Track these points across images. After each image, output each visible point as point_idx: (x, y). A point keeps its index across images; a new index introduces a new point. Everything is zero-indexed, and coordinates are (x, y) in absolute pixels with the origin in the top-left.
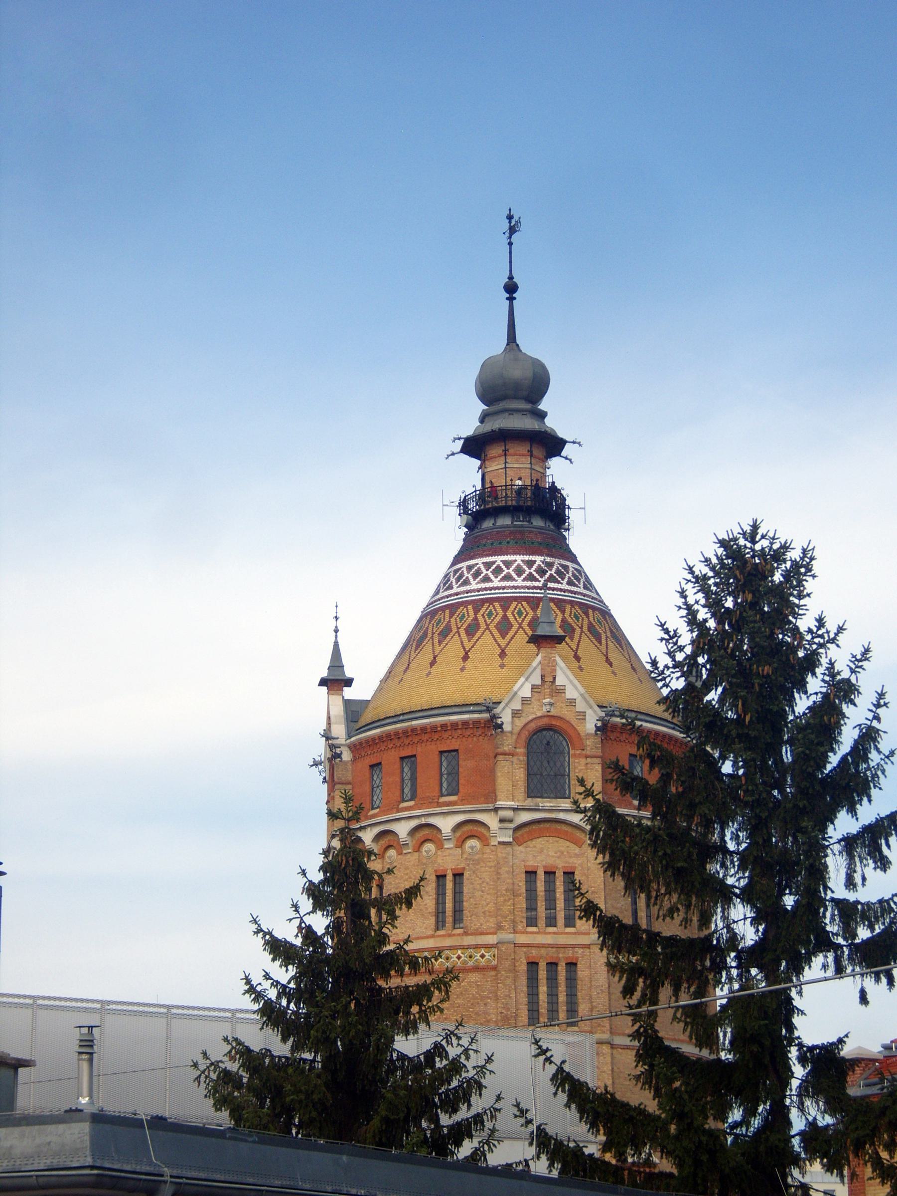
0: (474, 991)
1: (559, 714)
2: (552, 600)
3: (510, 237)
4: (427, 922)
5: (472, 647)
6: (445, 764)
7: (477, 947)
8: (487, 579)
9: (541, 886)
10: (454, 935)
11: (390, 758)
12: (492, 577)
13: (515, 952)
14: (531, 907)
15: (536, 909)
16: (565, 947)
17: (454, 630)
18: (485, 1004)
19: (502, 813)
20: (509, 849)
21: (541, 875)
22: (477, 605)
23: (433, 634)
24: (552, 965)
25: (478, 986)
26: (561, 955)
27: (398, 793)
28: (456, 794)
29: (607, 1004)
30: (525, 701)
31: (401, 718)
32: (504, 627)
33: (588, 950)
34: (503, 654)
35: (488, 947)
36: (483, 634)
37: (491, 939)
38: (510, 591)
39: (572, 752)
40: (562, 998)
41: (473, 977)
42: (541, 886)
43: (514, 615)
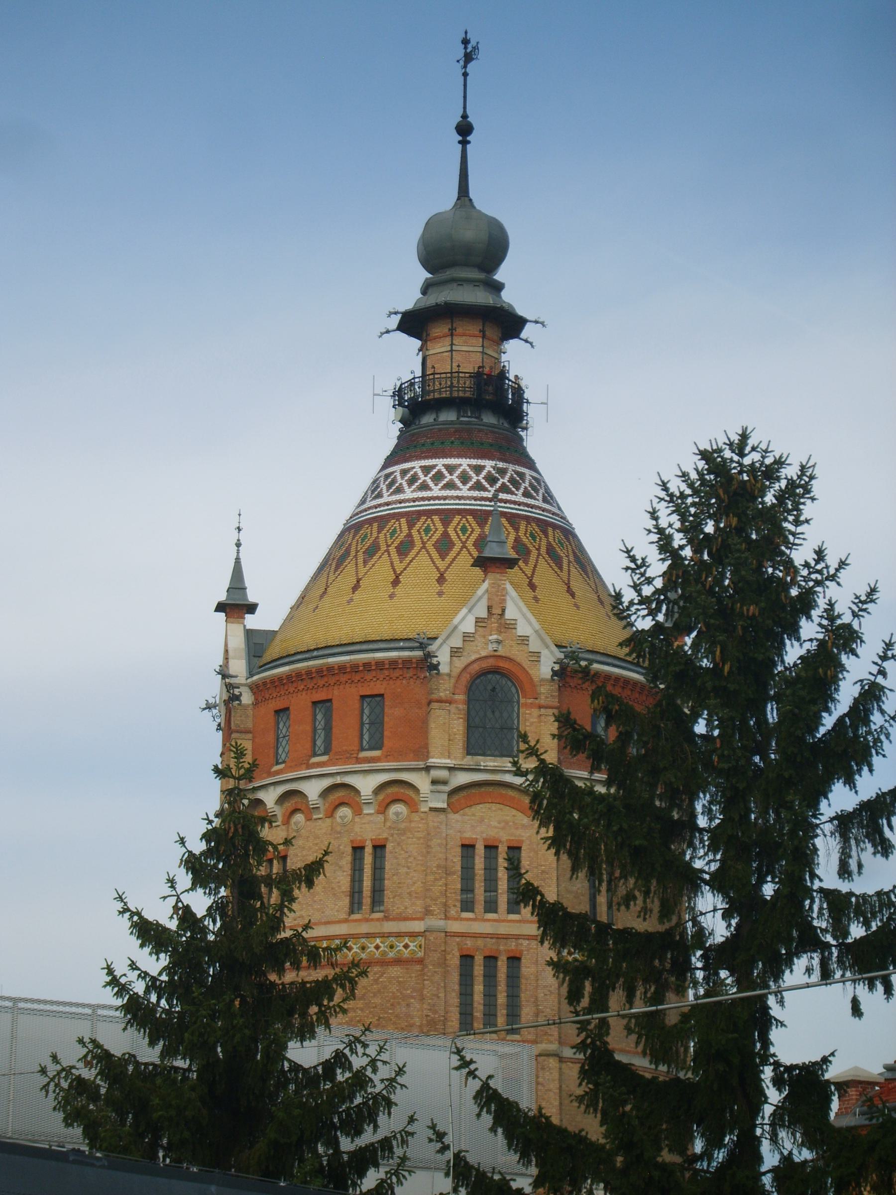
0: (394, 988)
1: (507, 655)
2: (504, 514)
3: (465, 67)
4: (340, 903)
5: (405, 569)
6: (367, 711)
7: (399, 935)
8: (424, 487)
9: (479, 863)
10: (372, 920)
11: (300, 702)
12: (431, 484)
13: (445, 942)
14: (467, 888)
15: (472, 891)
16: (507, 937)
17: (383, 548)
18: (408, 1005)
19: (435, 773)
20: (442, 816)
21: (480, 850)
22: (412, 518)
23: (357, 552)
24: (491, 960)
25: (399, 982)
26: (501, 948)
27: (308, 745)
28: (380, 748)
29: (556, 1008)
30: (466, 637)
31: (315, 653)
32: (444, 546)
34: (441, 579)
35: (413, 935)
36: (418, 553)
37: (418, 926)
38: (452, 502)
39: (522, 701)
40: (502, 999)
41: (395, 971)
42: (479, 863)
43: (456, 532)
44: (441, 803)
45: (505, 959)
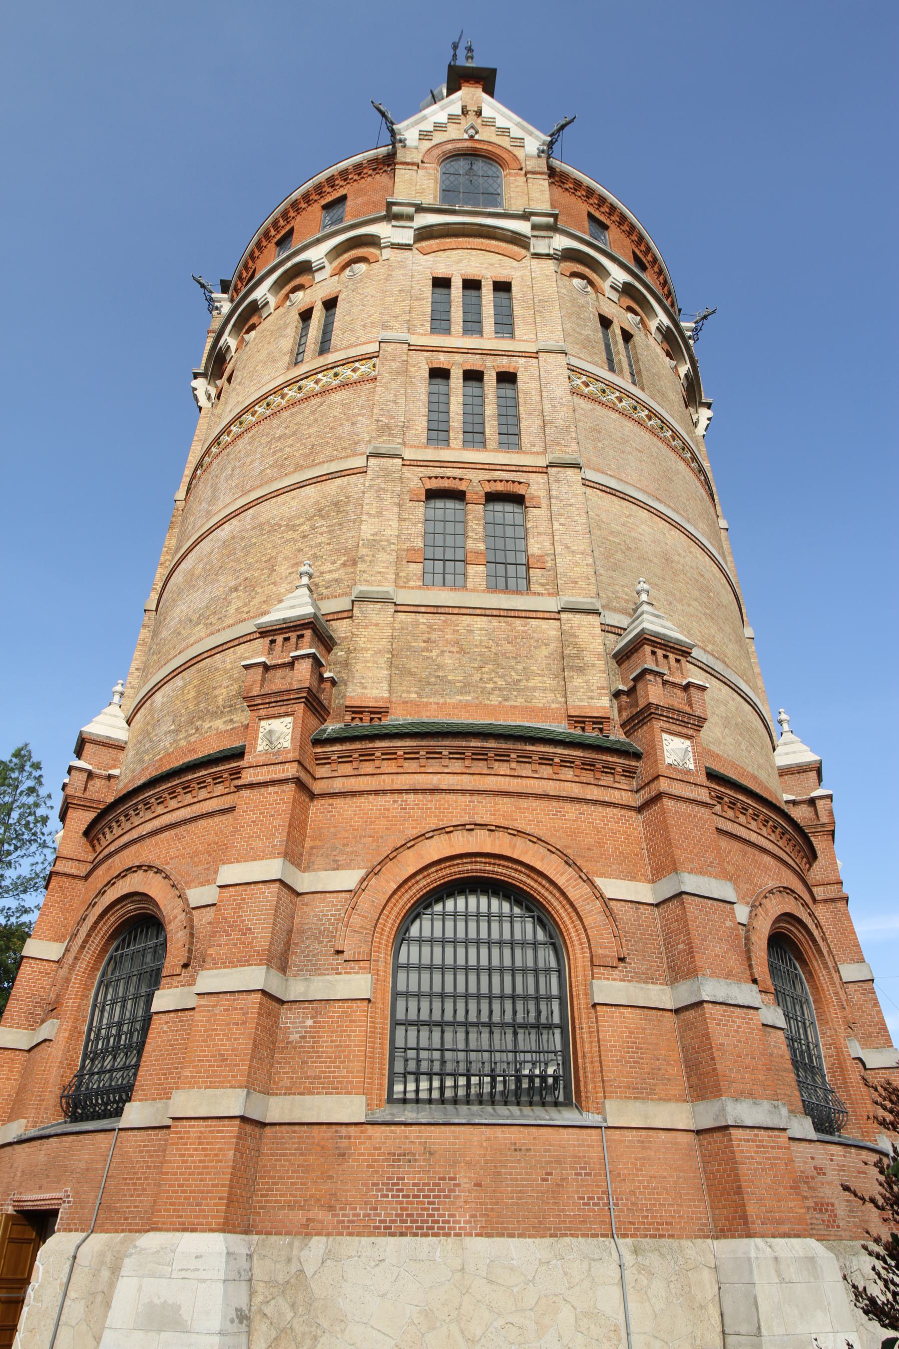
7: (345, 363)
20: (408, 254)
26: (488, 364)
30: (439, 127)
33: (536, 360)
41: (336, 397)
44: (406, 236)
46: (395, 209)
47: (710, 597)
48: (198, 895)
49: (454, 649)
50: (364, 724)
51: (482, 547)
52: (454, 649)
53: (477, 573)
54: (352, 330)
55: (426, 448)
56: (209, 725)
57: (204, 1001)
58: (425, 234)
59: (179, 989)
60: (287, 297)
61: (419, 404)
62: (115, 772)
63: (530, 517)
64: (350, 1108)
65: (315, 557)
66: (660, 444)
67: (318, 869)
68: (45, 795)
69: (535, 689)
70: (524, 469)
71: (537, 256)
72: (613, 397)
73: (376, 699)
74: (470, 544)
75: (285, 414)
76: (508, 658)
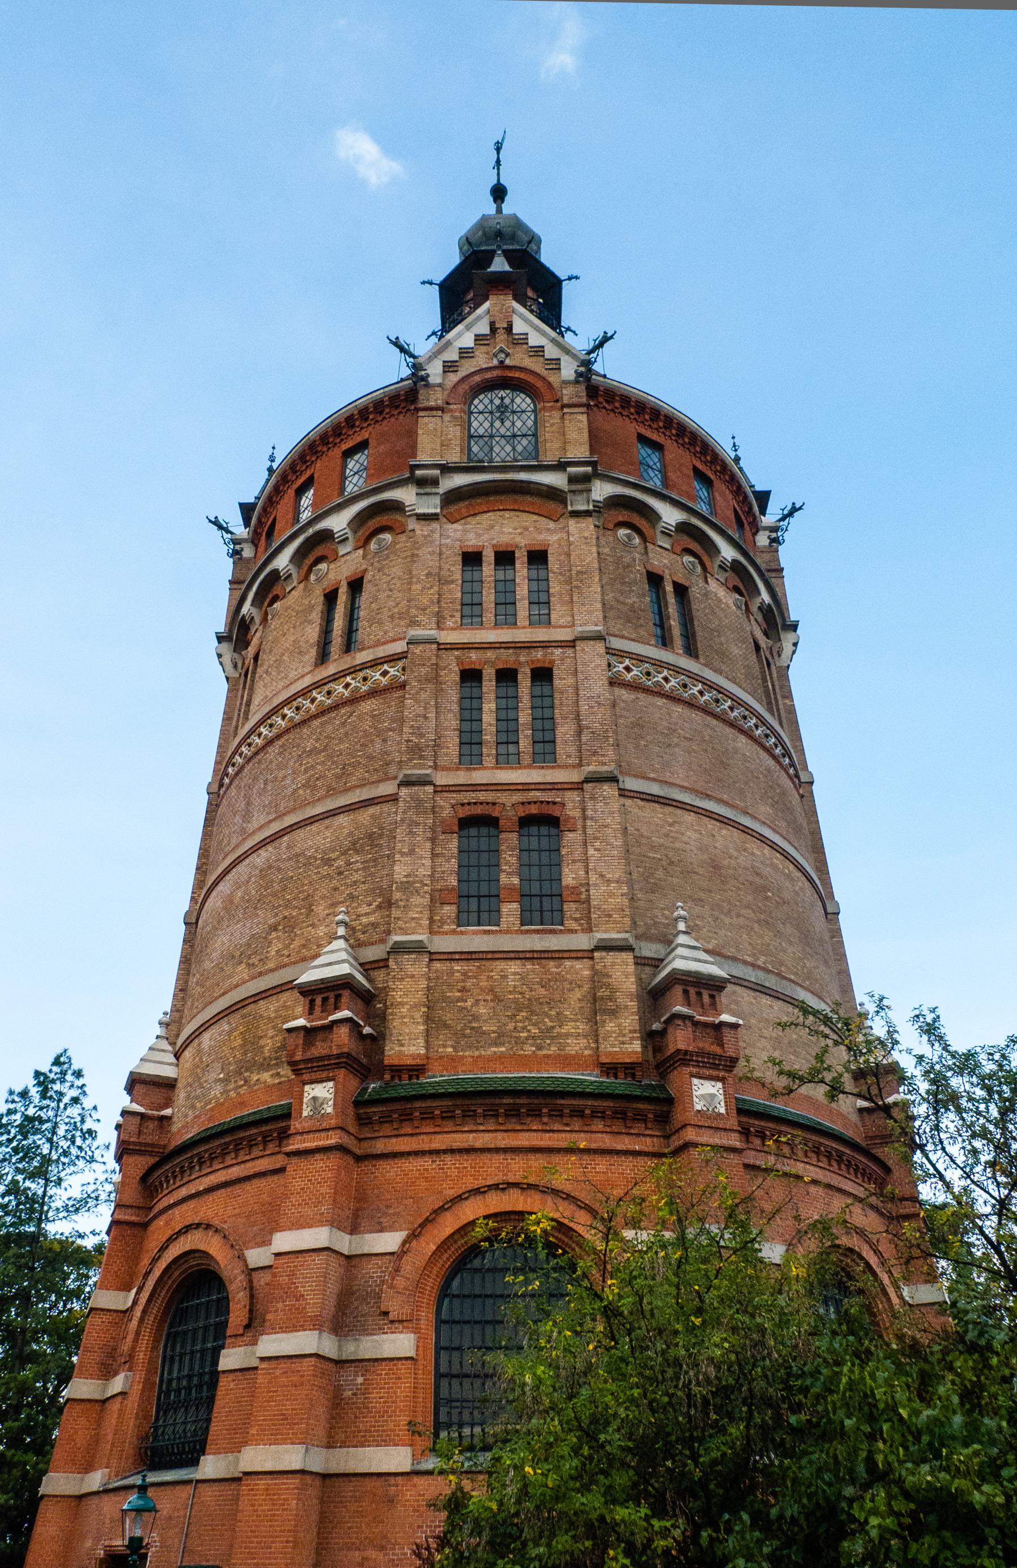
7: (375, 664)
16: (529, 646)
18: (385, 741)
20: (435, 525)
25: (373, 717)
26: (522, 659)
30: (465, 353)
35: (393, 659)
41: (366, 706)
44: (431, 506)
45: (528, 671)
46: (419, 473)
47: (767, 898)
48: (256, 1256)
49: (489, 998)
50: (405, 1087)
51: (516, 880)
52: (489, 998)
53: (510, 910)
54: (380, 623)
55: (458, 769)
56: (256, 1078)
57: (264, 1365)
58: (452, 498)
59: (242, 1349)
60: (310, 571)
61: (450, 715)
62: (168, 1112)
63: (564, 842)
64: (396, 1458)
65: (352, 897)
66: (714, 722)
67: (364, 1233)
68: (91, 1107)
69: (568, 1035)
70: (559, 786)
71: (576, 514)
72: (659, 678)
73: (413, 1056)
74: (504, 879)
75: (316, 723)
76: (541, 1004)
